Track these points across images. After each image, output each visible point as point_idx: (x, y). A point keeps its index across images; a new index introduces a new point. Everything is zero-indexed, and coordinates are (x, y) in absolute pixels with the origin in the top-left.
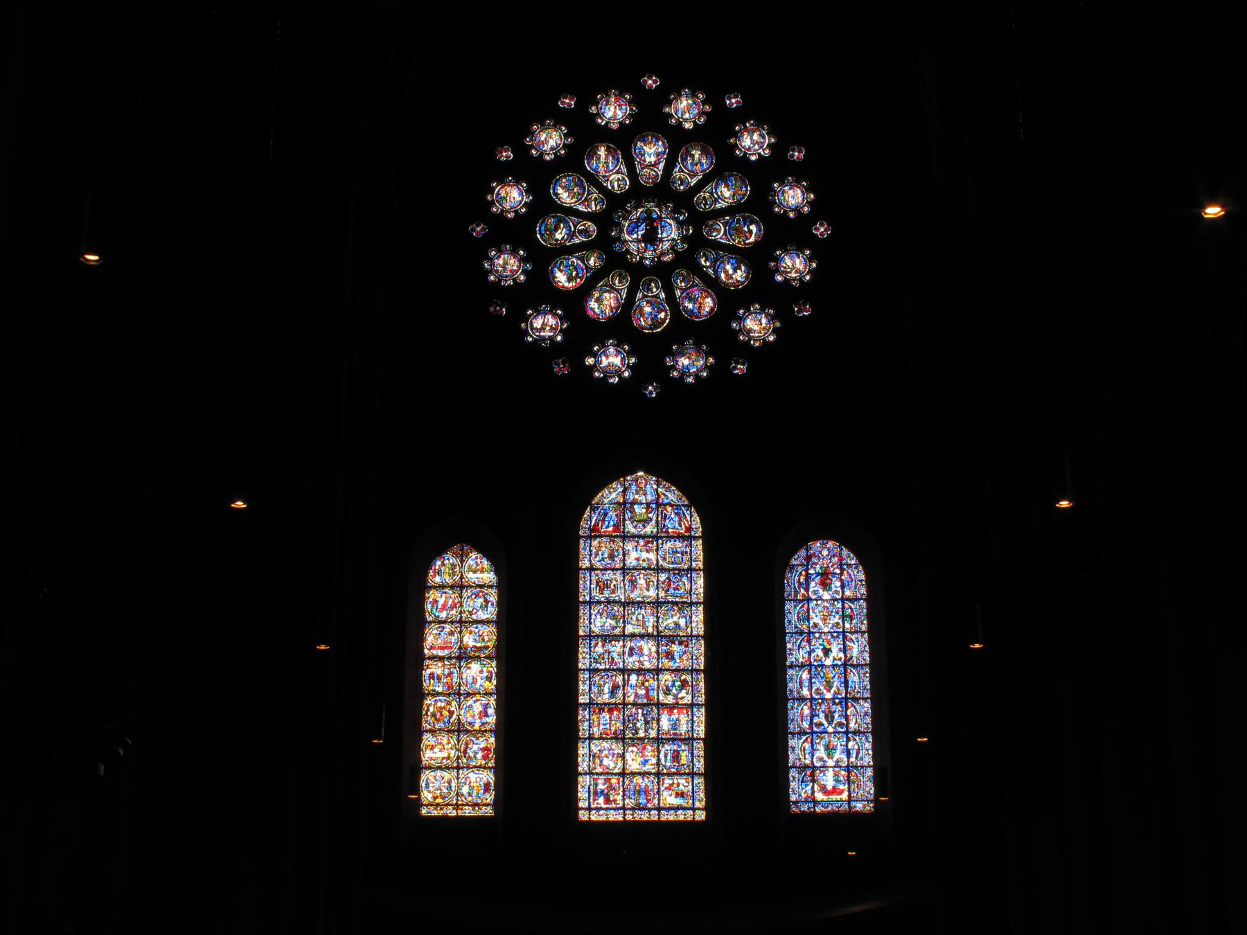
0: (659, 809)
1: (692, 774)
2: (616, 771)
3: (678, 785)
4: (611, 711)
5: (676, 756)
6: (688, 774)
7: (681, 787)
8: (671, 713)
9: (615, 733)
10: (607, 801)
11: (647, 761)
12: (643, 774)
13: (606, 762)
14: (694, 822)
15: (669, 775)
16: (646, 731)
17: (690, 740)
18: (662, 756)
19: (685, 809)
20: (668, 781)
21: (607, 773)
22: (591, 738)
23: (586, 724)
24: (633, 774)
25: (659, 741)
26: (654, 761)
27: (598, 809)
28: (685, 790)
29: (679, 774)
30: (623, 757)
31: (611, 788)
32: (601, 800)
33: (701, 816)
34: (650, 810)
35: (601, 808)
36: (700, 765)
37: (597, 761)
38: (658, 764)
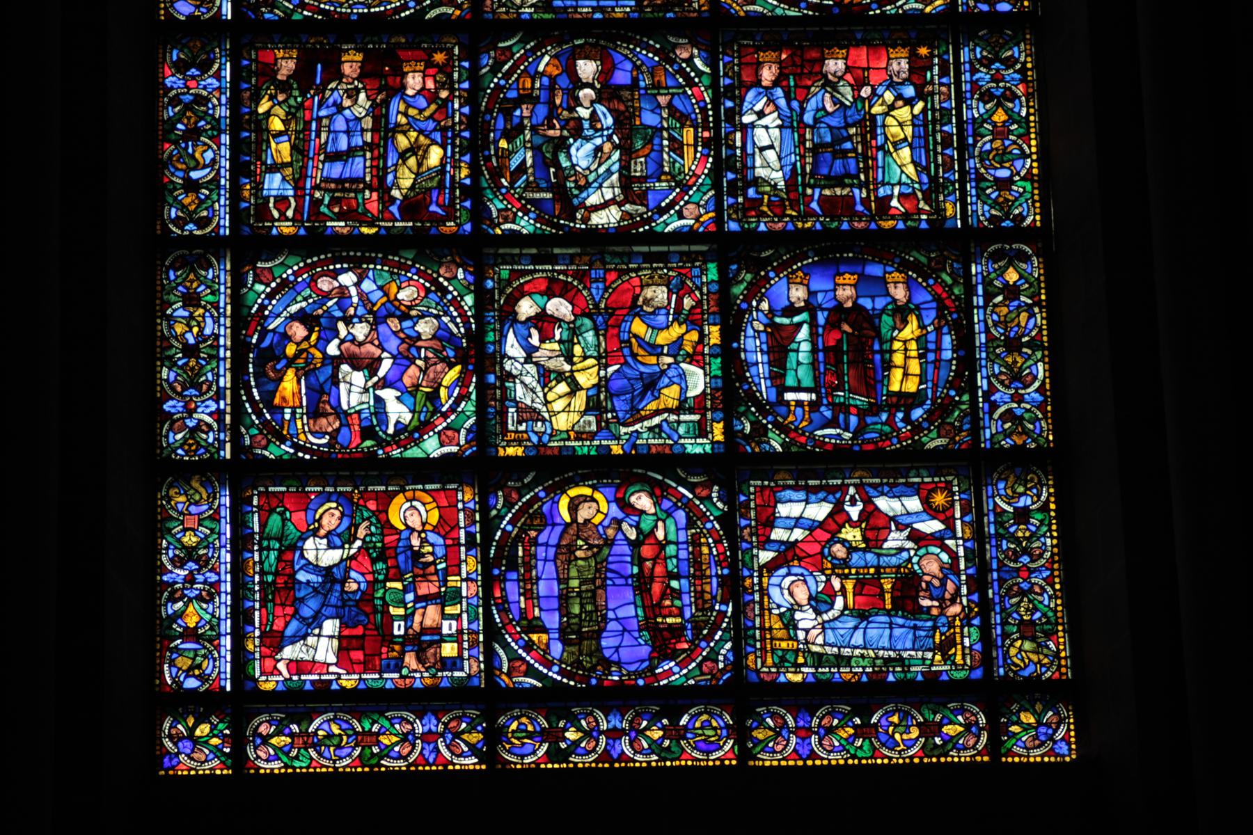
0: (742, 696)
1: (975, 465)
2: (431, 447)
3: (875, 525)
4: (383, 79)
5: (854, 347)
6: (938, 461)
7: (895, 539)
8: (801, 75)
9: (413, 205)
10: (367, 635)
11: (651, 385)
12: (617, 472)
13: (353, 390)
14: (996, 775)
15: (811, 467)
16: (630, 189)
17: (936, 247)
18: (753, 346)
19: (930, 693)
20: (799, 510)
21: (365, 468)
22: (250, 244)
23: (213, 157)
24: (557, 467)
25: (741, 249)
26: (697, 381)
27: (302, 702)
28: (931, 565)
29: (892, 465)
30: (478, 357)
31: (392, 554)
32: (323, 647)
33: (1041, 740)
34: (672, 702)
35: (324, 697)
36: (1020, 398)
37: (289, 384)
38: (731, 393)
